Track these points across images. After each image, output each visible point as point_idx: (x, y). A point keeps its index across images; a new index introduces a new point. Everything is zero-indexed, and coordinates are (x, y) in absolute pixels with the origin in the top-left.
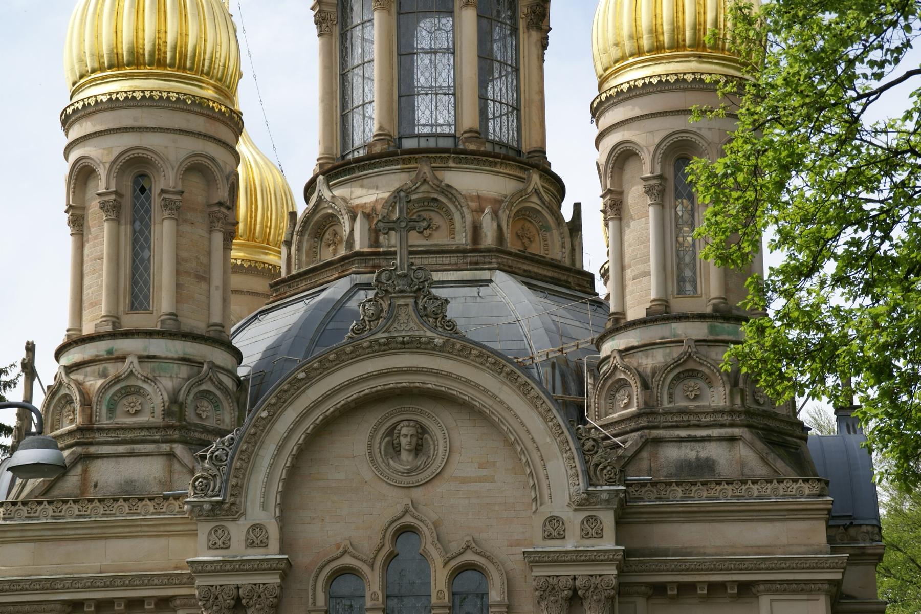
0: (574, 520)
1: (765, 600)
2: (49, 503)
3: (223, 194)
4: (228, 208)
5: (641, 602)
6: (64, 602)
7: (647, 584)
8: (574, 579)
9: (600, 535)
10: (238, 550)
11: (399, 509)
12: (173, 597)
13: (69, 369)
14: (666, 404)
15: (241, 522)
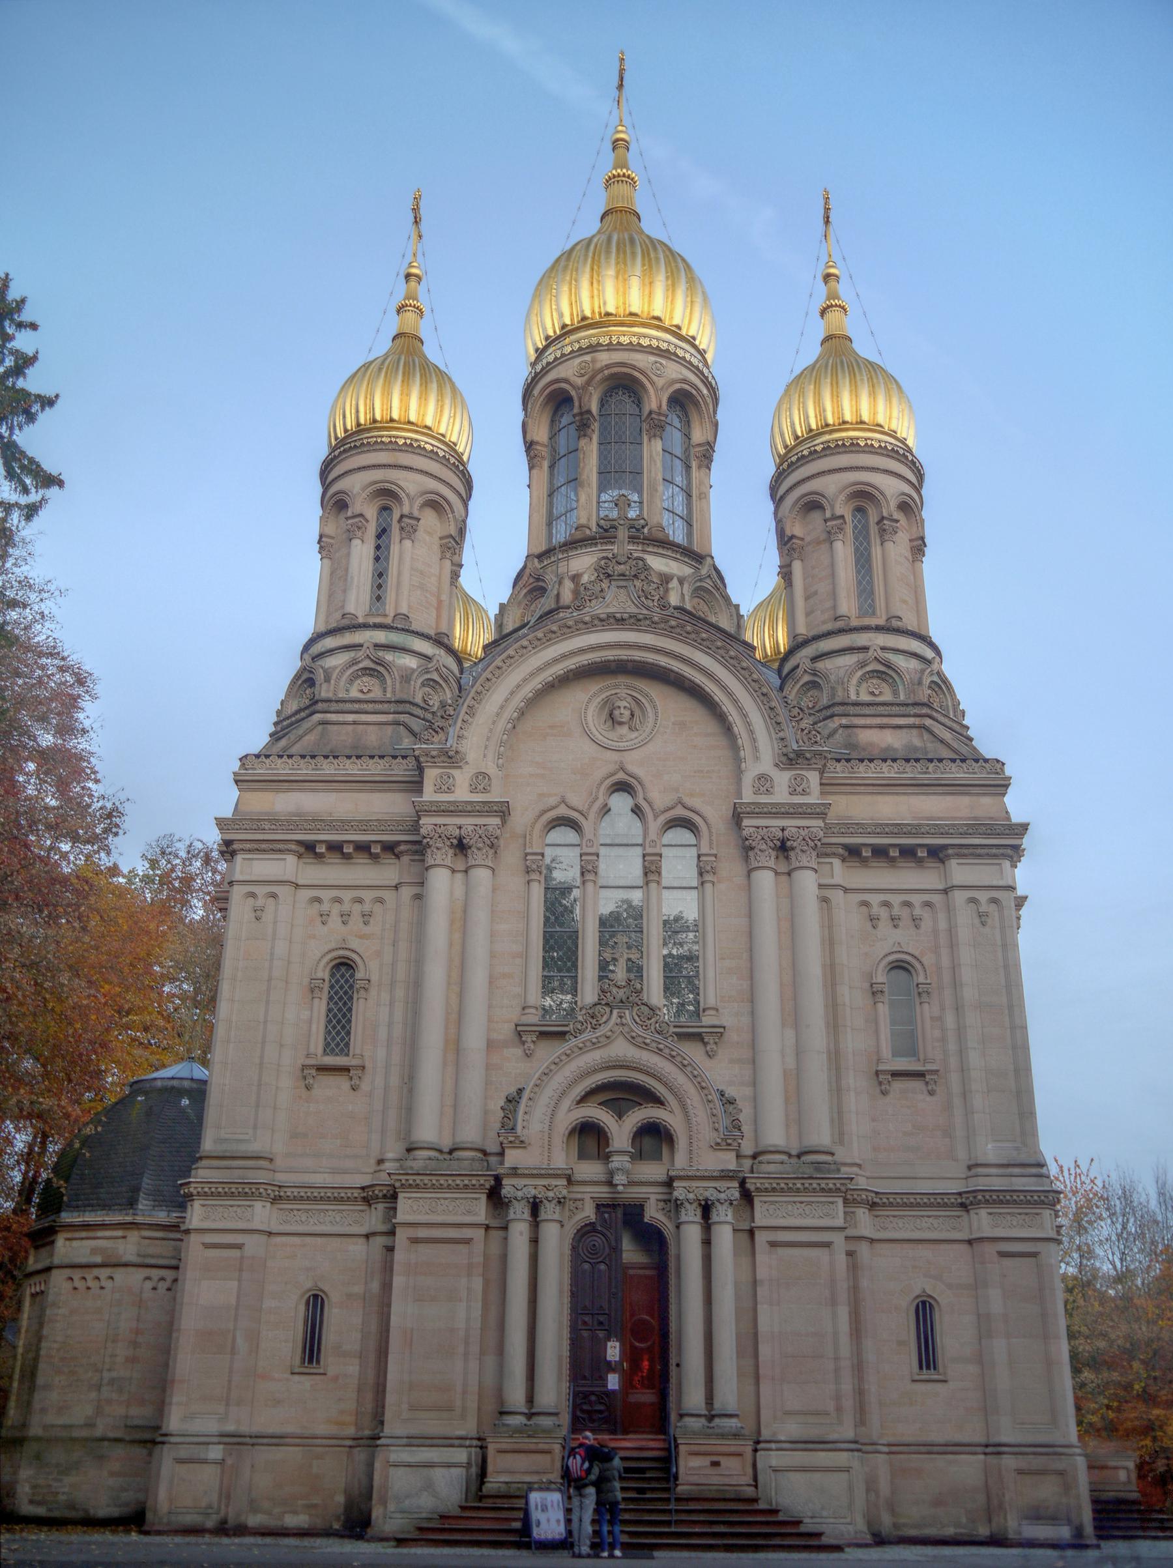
0: (782, 779)
1: (953, 863)
2: (290, 757)
3: (453, 531)
4: (457, 543)
5: (837, 862)
6: (299, 842)
7: (846, 847)
8: (783, 830)
9: (804, 792)
10: (462, 793)
11: (612, 768)
12: (399, 843)
13: (314, 658)
14: (853, 697)
15: (466, 768)
